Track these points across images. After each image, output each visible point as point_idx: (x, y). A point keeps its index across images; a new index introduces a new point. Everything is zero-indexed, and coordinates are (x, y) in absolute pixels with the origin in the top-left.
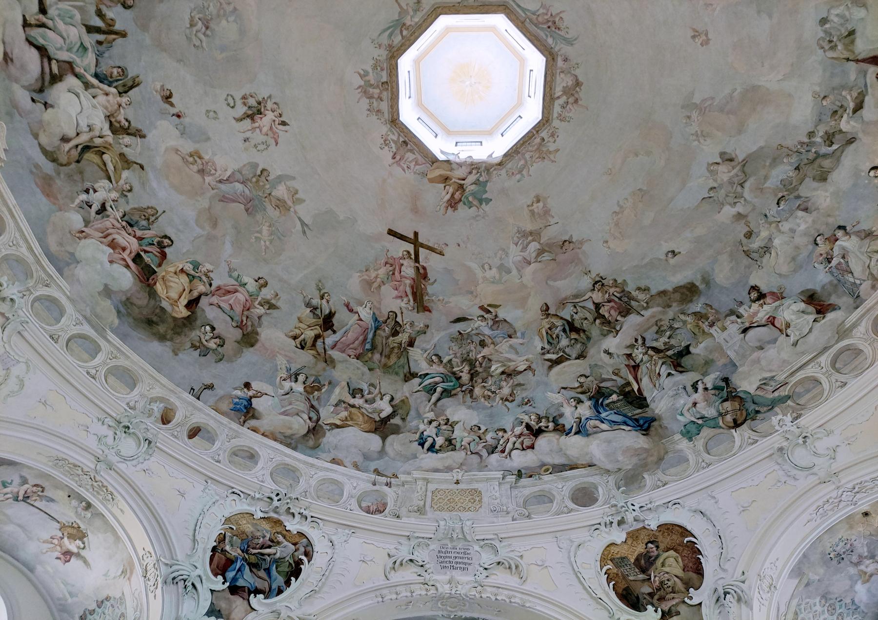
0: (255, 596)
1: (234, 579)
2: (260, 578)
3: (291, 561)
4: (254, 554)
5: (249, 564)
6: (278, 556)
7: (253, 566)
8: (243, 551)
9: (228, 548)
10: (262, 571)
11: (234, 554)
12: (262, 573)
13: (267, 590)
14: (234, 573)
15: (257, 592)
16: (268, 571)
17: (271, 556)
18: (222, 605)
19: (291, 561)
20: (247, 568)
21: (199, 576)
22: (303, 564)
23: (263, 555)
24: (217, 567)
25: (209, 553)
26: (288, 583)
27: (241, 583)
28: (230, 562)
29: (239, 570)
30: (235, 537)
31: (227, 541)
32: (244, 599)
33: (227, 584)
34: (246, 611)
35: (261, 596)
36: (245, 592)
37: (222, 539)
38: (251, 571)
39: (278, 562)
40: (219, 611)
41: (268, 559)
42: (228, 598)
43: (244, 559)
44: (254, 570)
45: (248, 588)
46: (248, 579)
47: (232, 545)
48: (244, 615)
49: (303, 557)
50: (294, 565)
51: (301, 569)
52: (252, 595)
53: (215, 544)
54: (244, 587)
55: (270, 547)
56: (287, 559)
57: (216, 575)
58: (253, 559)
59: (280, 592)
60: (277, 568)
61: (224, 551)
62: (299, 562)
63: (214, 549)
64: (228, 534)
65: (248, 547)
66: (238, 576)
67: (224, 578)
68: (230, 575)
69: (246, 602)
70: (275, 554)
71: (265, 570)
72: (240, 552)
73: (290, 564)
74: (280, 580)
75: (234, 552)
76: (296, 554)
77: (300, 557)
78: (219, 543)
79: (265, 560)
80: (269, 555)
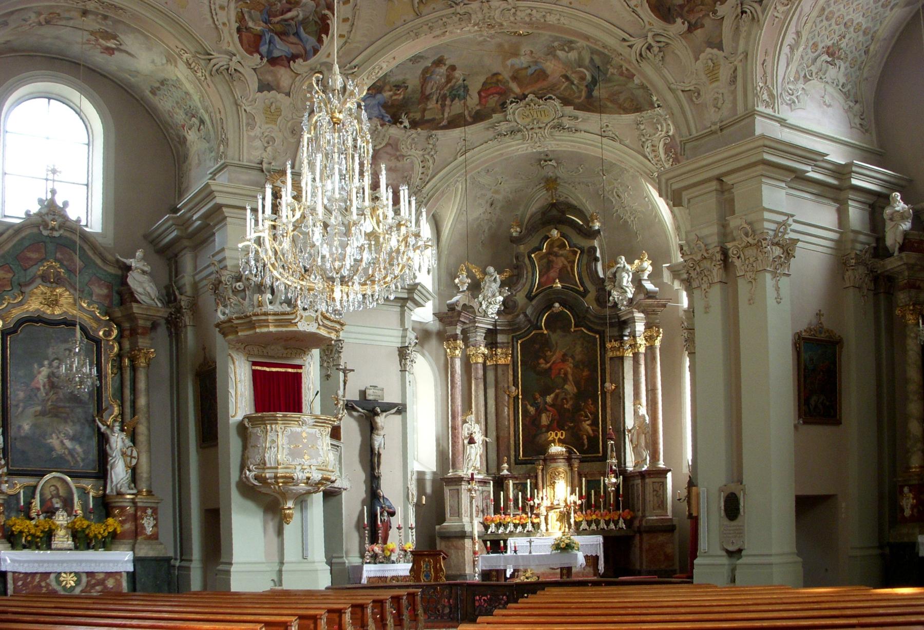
0: (294, 62)
1: (269, 52)
2: (292, 43)
3: (317, 20)
4: (278, 23)
5: (276, 34)
6: (301, 16)
7: (282, 34)
8: (266, 23)
9: (251, 24)
10: (292, 36)
11: (259, 28)
12: (293, 39)
13: (303, 52)
14: (267, 46)
15: (294, 57)
16: (297, 34)
17: (296, 19)
18: (269, 78)
19: (317, 20)
20: (276, 38)
21: (239, 62)
22: (328, 19)
23: (286, 20)
24: (249, 46)
25: (236, 36)
26: (320, 41)
27: (276, 54)
28: (259, 37)
29: (270, 42)
30: (252, 11)
31: (246, 17)
32: (285, 67)
33: (265, 60)
34: (291, 77)
35: (299, 61)
36: (283, 60)
37: (241, 18)
38: (281, 39)
39: (304, 22)
40: (268, 84)
41: (293, 23)
42: (272, 71)
43: (272, 31)
44: (284, 38)
45: (286, 56)
46: (281, 48)
47: (253, 20)
48: (291, 81)
49: (326, 12)
50: (319, 22)
51: (328, 25)
52: (292, 62)
53: (237, 25)
54: (281, 56)
55: (290, 10)
56: (311, 18)
57: (251, 53)
58: (279, 28)
59: (316, 51)
60: (304, 30)
61: (248, 29)
62: (324, 19)
63: (239, 30)
64: (245, 10)
65: (269, 17)
66: (271, 48)
67: (260, 54)
68: (264, 49)
69: (288, 70)
70: (297, 16)
71: (294, 34)
72: (264, 25)
73: (316, 22)
74: (312, 41)
75: (257, 27)
76: (318, 9)
77: (323, 12)
78: (240, 22)
79: (290, 25)
80: (292, 19)
